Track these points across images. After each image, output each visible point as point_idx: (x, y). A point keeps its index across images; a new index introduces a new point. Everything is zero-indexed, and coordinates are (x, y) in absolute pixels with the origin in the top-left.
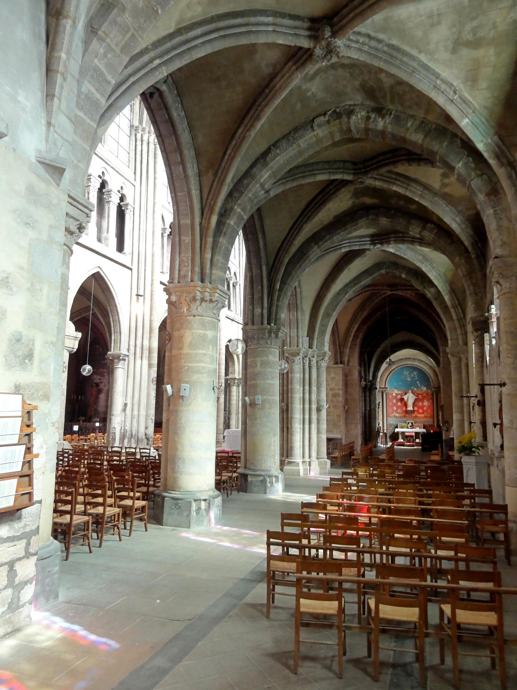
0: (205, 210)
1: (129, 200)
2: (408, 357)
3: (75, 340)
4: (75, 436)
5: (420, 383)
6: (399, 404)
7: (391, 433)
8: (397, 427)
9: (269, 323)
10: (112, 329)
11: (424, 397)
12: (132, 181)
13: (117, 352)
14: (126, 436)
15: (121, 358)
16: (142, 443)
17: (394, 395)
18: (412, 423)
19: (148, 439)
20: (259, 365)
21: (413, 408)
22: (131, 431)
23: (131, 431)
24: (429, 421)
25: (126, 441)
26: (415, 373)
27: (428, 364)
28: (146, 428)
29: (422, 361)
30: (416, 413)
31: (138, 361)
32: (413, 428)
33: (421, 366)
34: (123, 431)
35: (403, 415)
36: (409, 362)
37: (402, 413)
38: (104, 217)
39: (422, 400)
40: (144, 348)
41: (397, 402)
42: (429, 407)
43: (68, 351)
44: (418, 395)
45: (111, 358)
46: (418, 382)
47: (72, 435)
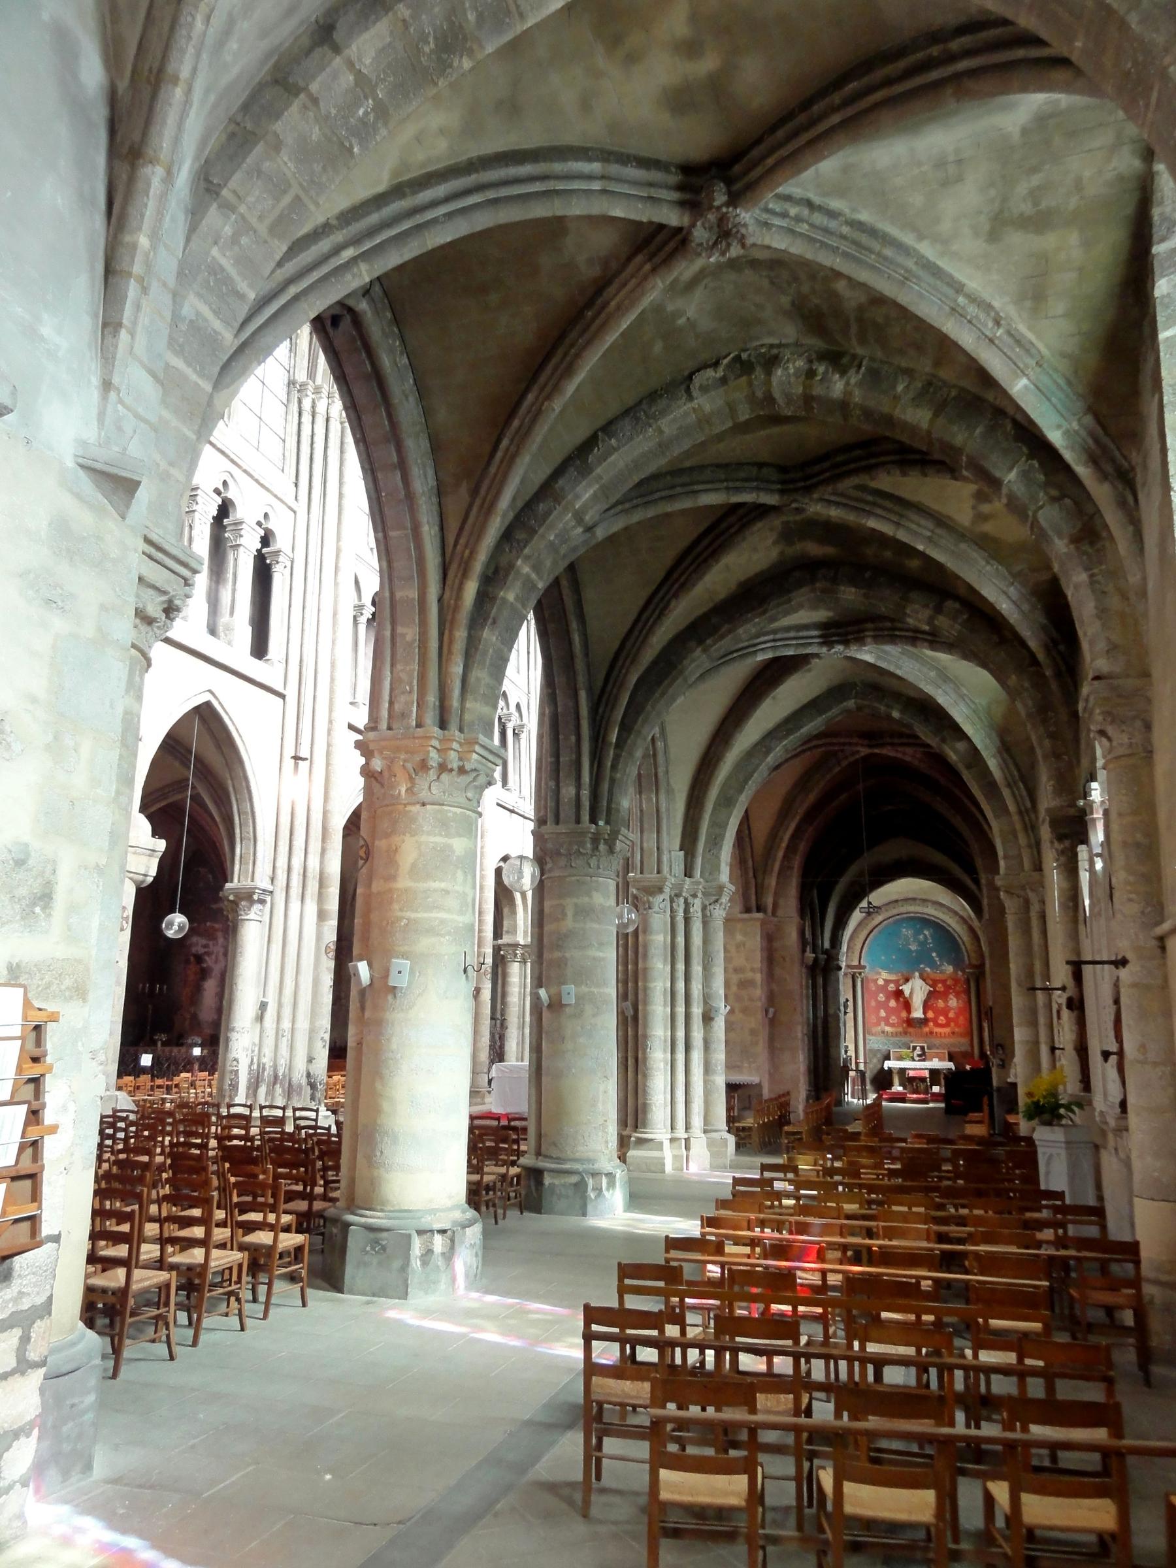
0: (451, 568)
1: (281, 542)
2: (911, 896)
3: (150, 856)
4: (145, 1079)
5: (938, 955)
6: (893, 1003)
7: (875, 1071)
8: (888, 1058)
9: (593, 820)
10: (237, 831)
11: (948, 988)
12: (290, 500)
13: (247, 883)
14: (263, 1080)
15: (256, 897)
16: (299, 1094)
17: (881, 982)
18: (922, 1048)
19: (313, 1086)
20: (570, 913)
21: (925, 1013)
22: (275, 1067)
23: (275, 1067)
24: (961, 1044)
25: (262, 1090)
26: (926, 932)
27: (956, 913)
28: (310, 1060)
30: (931, 1024)
31: (295, 905)
32: (924, 1060)
34: (255, 1067)
35: (900, 1029)
36: (912, 908)
37: (899, 1025)
38: (225, 580)
39: (944, 996)
40: (310, 874)
41: (888, 999)
42: (959, 1012)
43: (135, 882)
44: (933, 983)
45: (231, 898)
46: (934, 954)
47: (137, 1076)
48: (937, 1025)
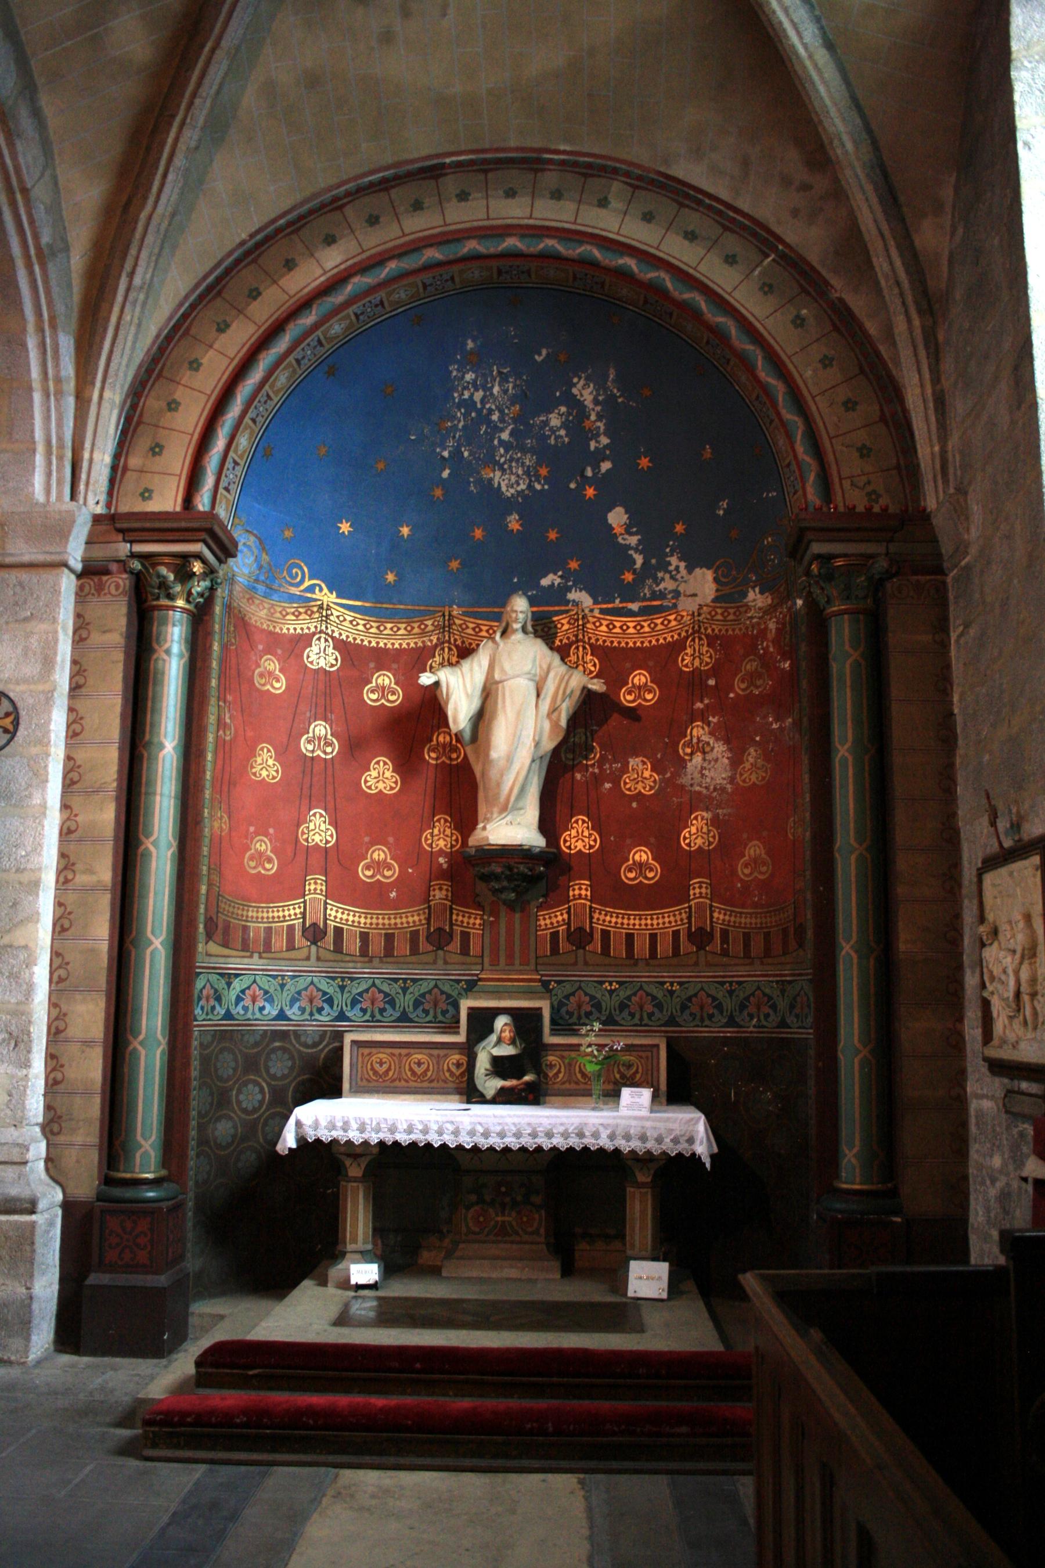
2: (517, 135)
6: (380, 777)
17: (321, 657)
18: (526, 1023)
21: (548, 824)
26: (585, 393)
27: (761, 237)
29: (683, 195)
30: (581, 890)
32: (531, 1096)
33: (678, 250)
35: (412, 919)
36: (514, 210)
37: (412, 893)
41: (355, 749)
42: (744, 814)
44: (614, 662)
46: (617, 518)
48: (615, 893)
